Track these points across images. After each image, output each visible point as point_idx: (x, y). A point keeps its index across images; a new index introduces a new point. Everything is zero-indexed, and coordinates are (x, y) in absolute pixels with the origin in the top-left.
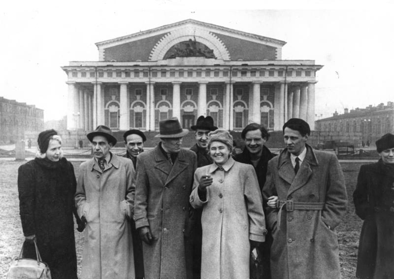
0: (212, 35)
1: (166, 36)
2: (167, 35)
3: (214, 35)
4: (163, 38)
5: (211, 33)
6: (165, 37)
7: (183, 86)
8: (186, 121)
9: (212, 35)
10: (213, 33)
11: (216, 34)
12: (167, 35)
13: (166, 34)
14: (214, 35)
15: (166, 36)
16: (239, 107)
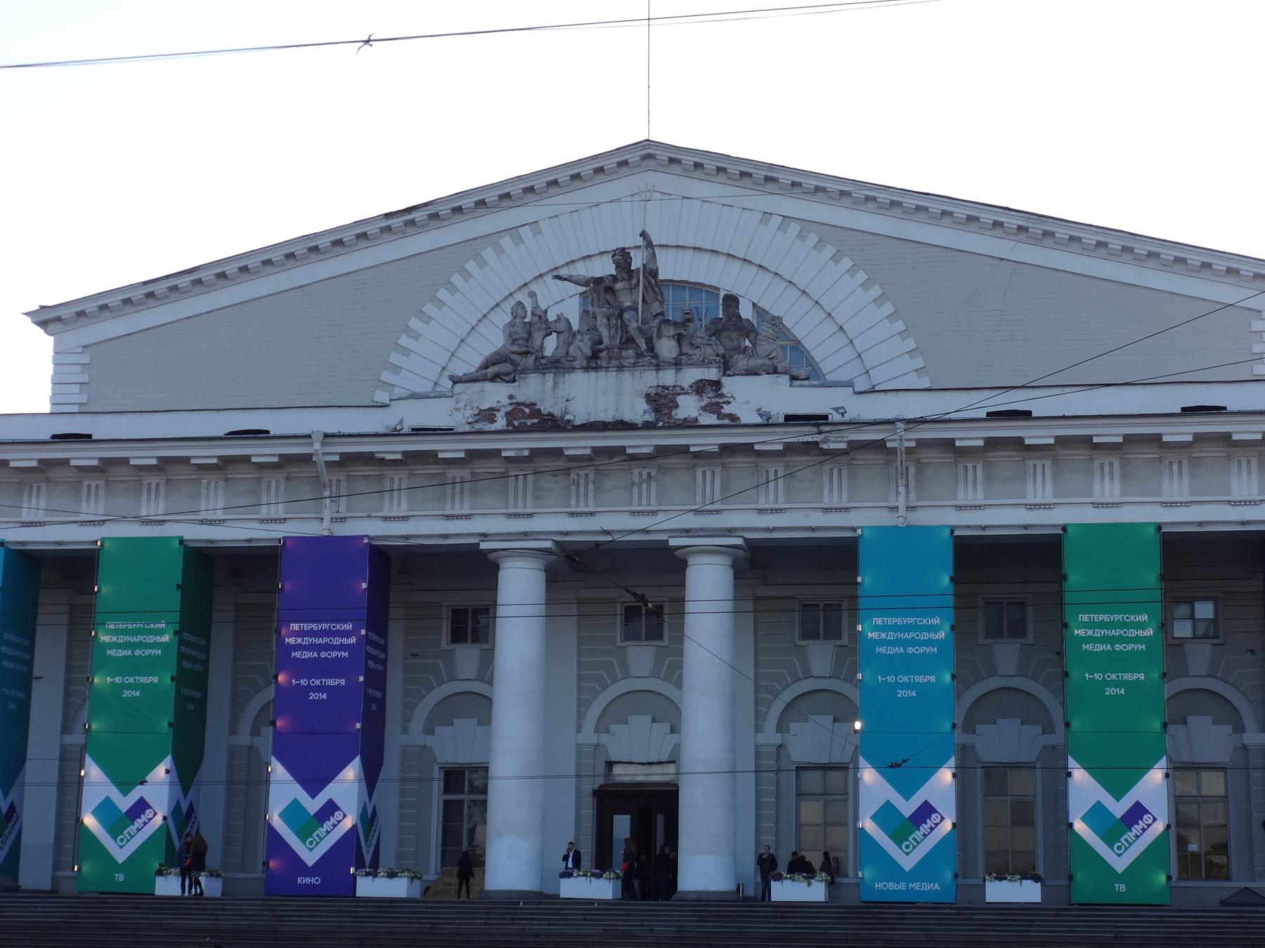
0: (801, 236)
1: (488, 254)
2: (500, 251)
3: (813, 239)
4: (471, 266)
5: (794, 228)
6: (482, 263)
7: (577, 570)
8: (622, 825)
9: (801, 236)
10: (807, 225)
11: (827, 233)
12: (500, 251)
13: (491, 238)
14: (813, 239)
15: (488, 254)
16: (1009, 726)
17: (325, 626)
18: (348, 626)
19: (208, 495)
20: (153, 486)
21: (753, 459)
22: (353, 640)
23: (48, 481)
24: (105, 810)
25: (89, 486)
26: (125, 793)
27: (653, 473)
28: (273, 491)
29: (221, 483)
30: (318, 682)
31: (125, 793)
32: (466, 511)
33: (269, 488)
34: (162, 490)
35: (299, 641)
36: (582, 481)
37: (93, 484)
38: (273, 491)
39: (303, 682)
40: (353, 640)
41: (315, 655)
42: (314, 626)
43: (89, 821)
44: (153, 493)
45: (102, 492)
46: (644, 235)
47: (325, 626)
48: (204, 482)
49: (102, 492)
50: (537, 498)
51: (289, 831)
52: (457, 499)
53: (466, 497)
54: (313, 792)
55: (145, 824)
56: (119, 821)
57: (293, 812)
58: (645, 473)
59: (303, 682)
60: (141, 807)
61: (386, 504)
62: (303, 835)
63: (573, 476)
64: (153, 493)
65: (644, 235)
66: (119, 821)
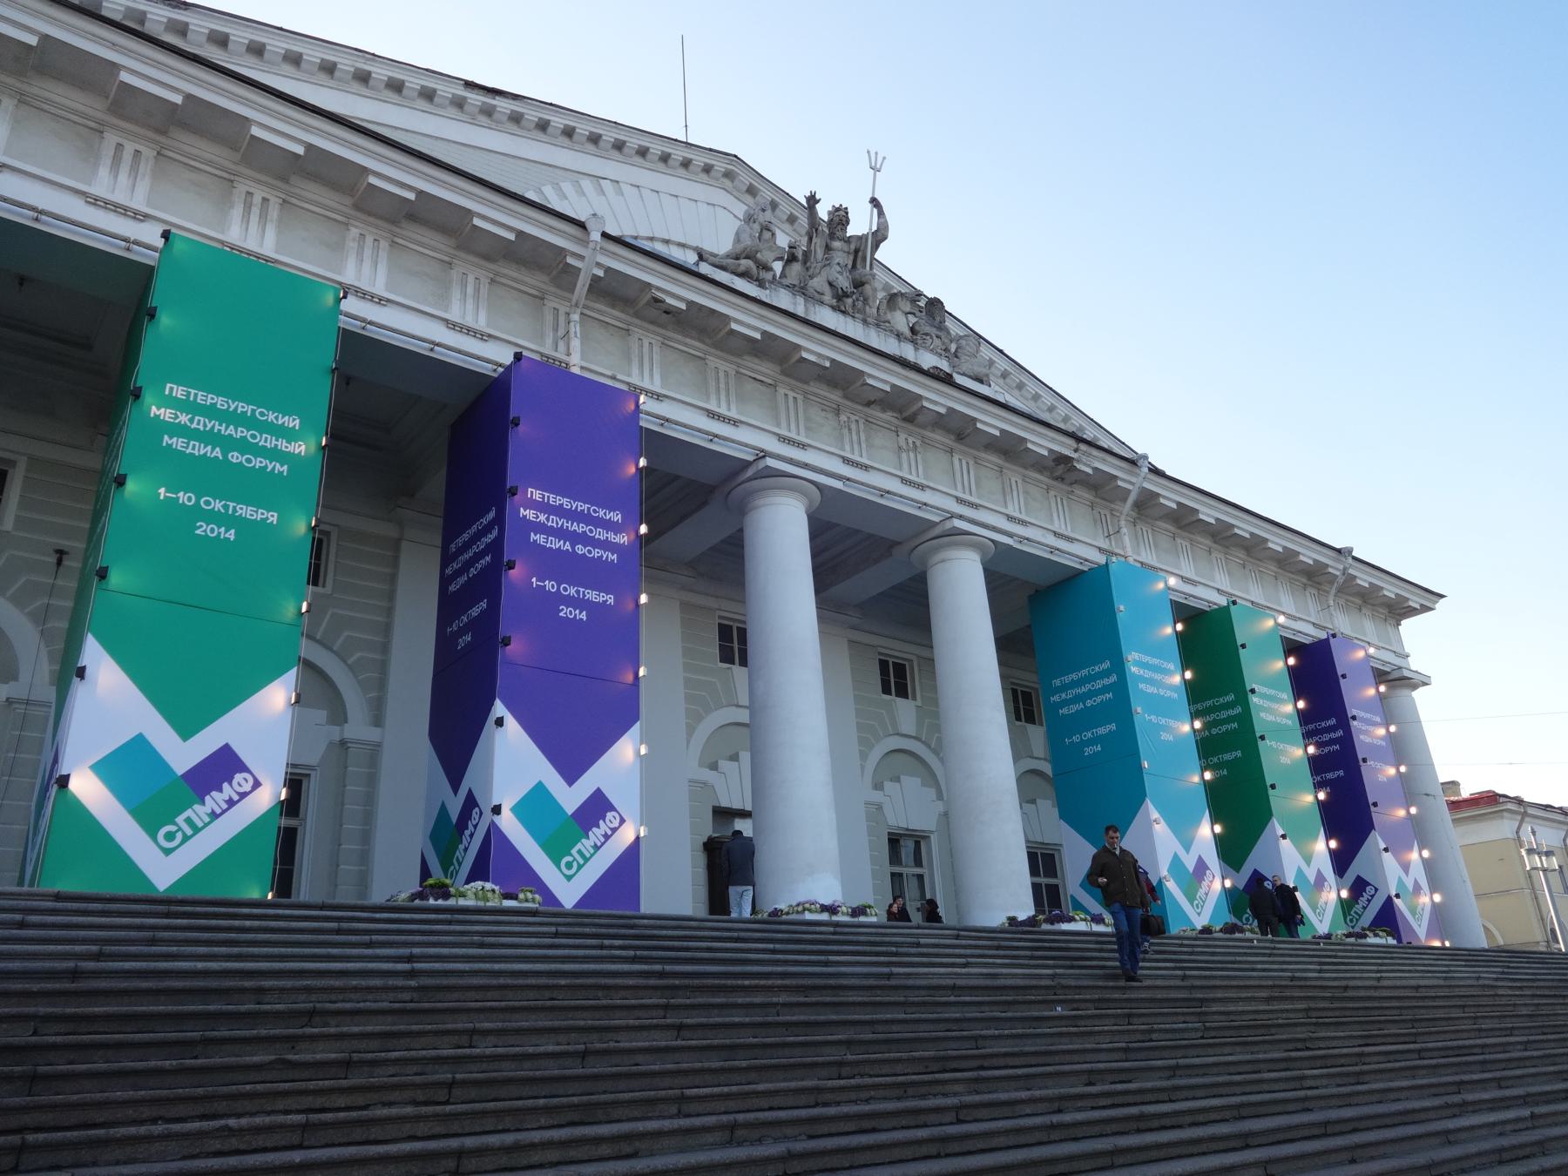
17: (582, 507)
18: (616, 517)
19: (360, 253)
20: (257, 199)
21: (1000, 462)
22: (623, 539)
23: (23, 99)
24: (129, 765)
25: (119, 146)
26: (186, 733)
27: (918, 443)
28: (470, 290)
29: (384, 244)
30: (572, 591)
31: (186, 733)
32: (733, 414)
33: (464, 285)
34: (274, 212)
35: (542, 518)
36: (853, 426)
37: (130, 148)
38: (470, 290)
39: (549, 585)
40: (623, 539)
41: (568, 546)
42: (565, 502)
43: (85, 786)
44: (255, 211)
45: (146, 167)
46: (875, 202)
47: (582, 507)
48: (354, 232)
49: (146, 167)
50: (808, 429)
51: (531, 840)
52: (723, 397)
53: (733, 398)
54: (571, 774)
55: (231, 803)
56: (160, 796)
57: (536, 804)
58: (910, 441)
59: (549, 585)
60: (222, 767)
61: (635, 370)
62: (556, 851)
63: (843, 418)
64: (255, 211)
65: (875, 202)
66: (160, 796)
